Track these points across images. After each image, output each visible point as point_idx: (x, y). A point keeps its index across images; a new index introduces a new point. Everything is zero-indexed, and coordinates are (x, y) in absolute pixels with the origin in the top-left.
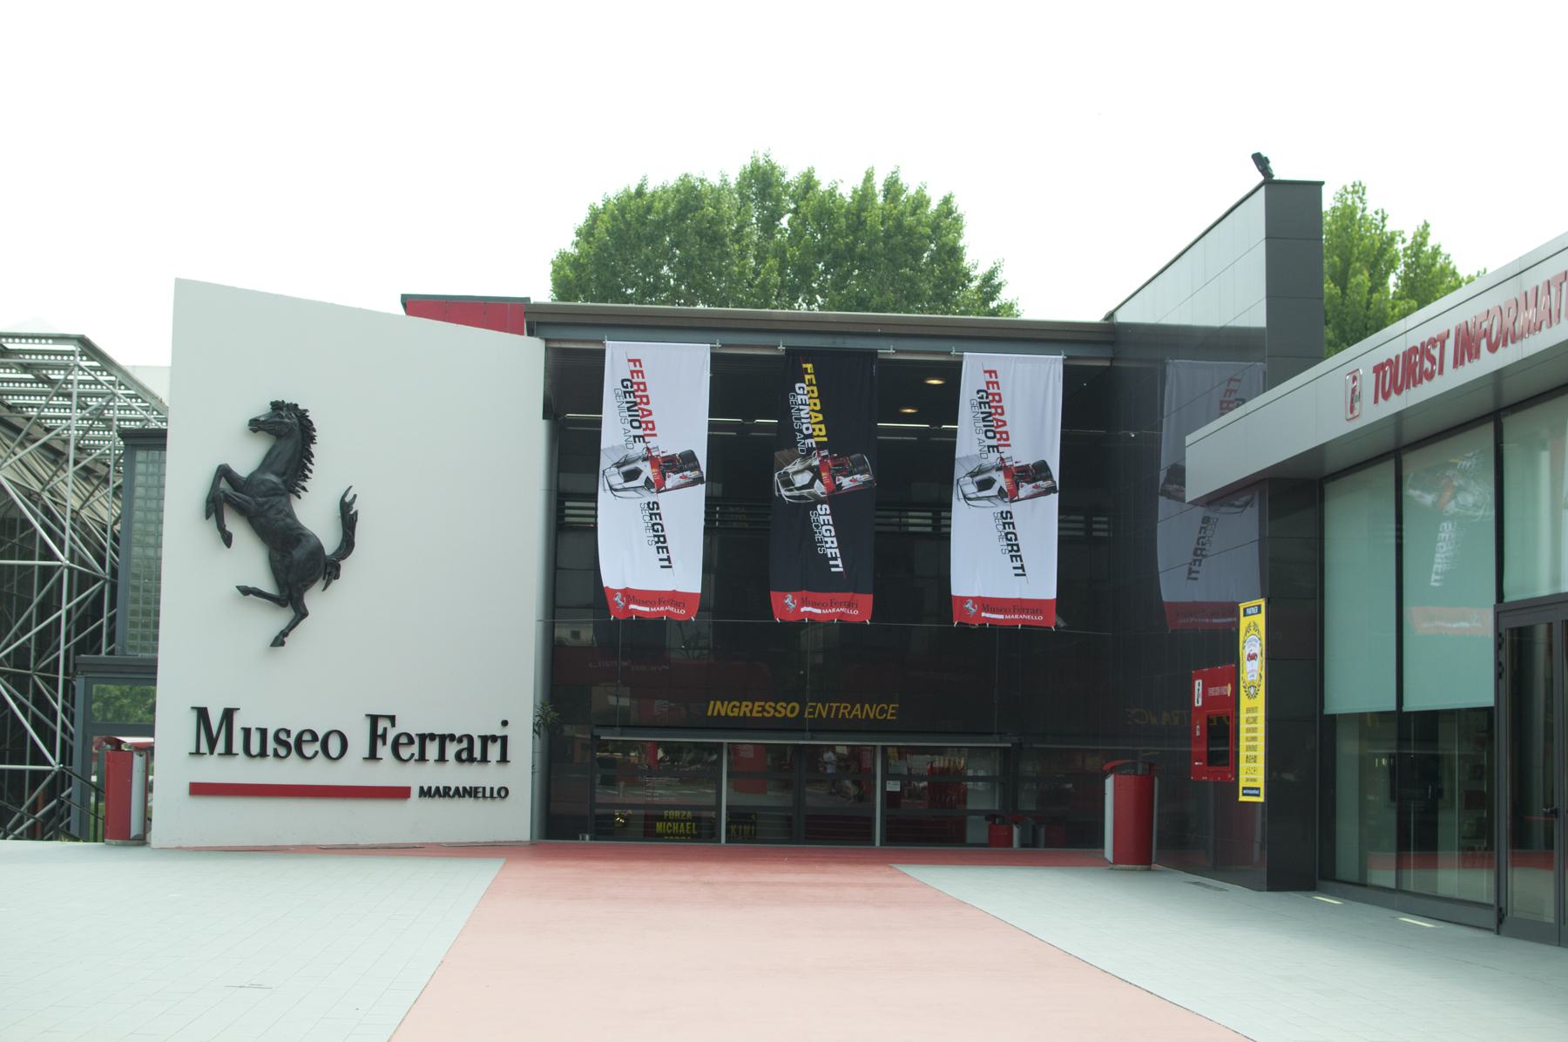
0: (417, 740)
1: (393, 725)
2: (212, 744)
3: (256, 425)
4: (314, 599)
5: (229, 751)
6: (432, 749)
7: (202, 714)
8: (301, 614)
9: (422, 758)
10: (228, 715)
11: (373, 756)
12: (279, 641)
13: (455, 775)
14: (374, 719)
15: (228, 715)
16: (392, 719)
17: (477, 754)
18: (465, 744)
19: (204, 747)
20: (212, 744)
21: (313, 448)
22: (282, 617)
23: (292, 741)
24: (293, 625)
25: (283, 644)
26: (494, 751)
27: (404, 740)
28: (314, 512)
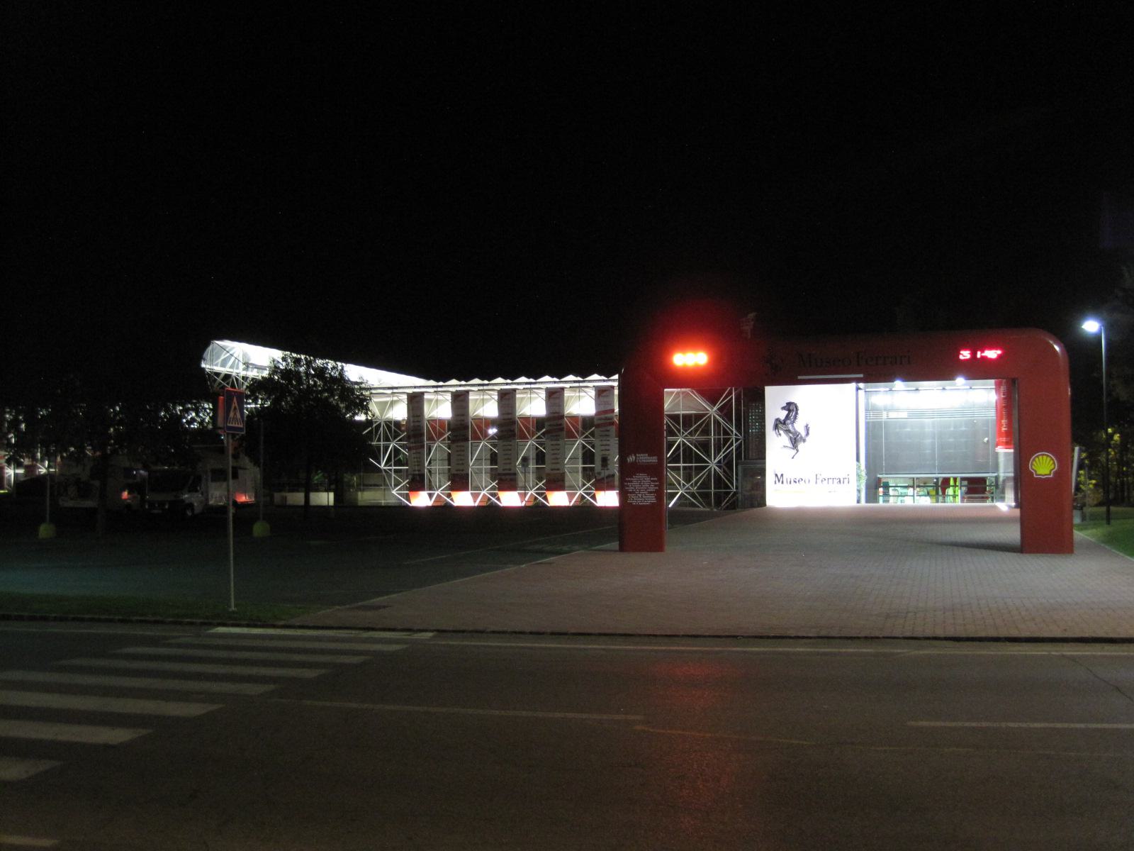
2: (779, 481)
3: (783, 408)
4: (801, 446)
7: (776, 475)
8: (798, 451)
10: (782, 475)
15: (782, 475)
17: (842, 482)
19: (777, 482)
20: (779, 481)
28: (799, 426)
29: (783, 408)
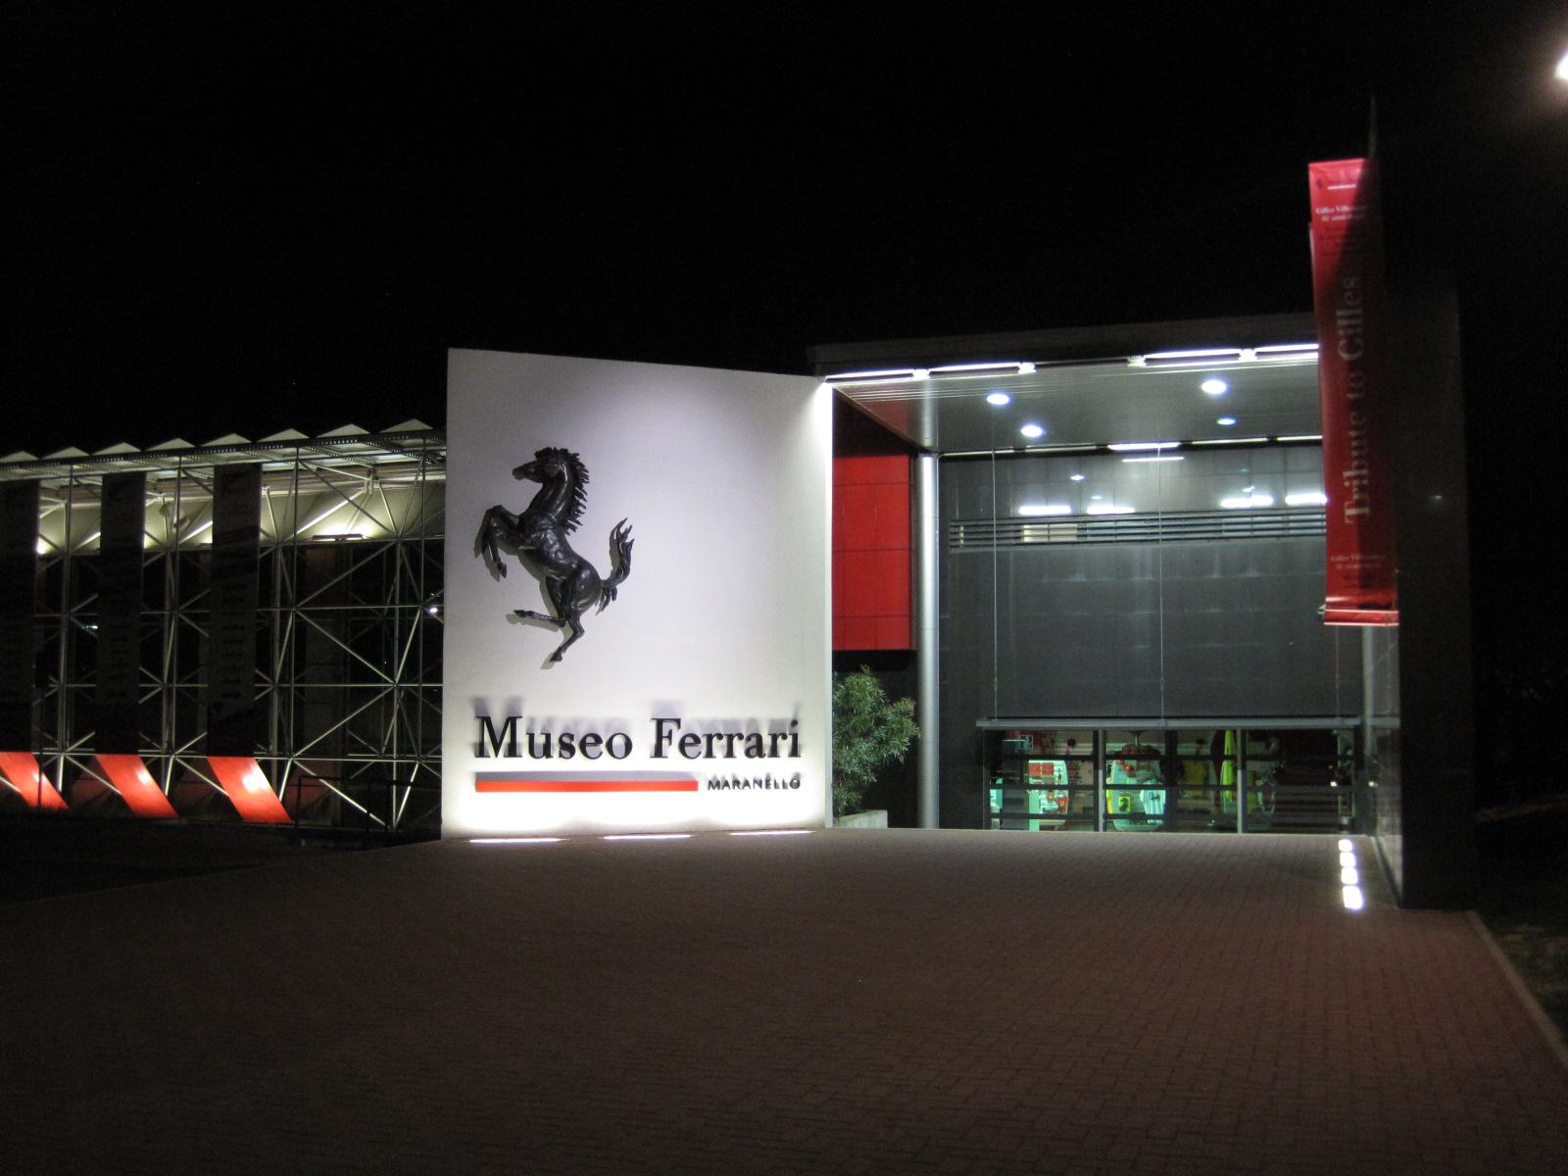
0: (704, 741)
1: (679, 727)
4: (589, 618)
5: (512, 751)
6: (719, 746)
7: (486, 721)
8: (577, 632)
9: (709, 754)
10: (511, 721)
11: (658, 752)
12: (556, 657)
13: (743, 766)
14: (660, 723)
16: (678, 722)
18: (754, 740)
21: (586, 487)
22: (558, 637)
23: (576, 744)
25: (560, 659)
26: (785, 746)
27: (689, 740)
28: (589, 542)
29: (522, 472)
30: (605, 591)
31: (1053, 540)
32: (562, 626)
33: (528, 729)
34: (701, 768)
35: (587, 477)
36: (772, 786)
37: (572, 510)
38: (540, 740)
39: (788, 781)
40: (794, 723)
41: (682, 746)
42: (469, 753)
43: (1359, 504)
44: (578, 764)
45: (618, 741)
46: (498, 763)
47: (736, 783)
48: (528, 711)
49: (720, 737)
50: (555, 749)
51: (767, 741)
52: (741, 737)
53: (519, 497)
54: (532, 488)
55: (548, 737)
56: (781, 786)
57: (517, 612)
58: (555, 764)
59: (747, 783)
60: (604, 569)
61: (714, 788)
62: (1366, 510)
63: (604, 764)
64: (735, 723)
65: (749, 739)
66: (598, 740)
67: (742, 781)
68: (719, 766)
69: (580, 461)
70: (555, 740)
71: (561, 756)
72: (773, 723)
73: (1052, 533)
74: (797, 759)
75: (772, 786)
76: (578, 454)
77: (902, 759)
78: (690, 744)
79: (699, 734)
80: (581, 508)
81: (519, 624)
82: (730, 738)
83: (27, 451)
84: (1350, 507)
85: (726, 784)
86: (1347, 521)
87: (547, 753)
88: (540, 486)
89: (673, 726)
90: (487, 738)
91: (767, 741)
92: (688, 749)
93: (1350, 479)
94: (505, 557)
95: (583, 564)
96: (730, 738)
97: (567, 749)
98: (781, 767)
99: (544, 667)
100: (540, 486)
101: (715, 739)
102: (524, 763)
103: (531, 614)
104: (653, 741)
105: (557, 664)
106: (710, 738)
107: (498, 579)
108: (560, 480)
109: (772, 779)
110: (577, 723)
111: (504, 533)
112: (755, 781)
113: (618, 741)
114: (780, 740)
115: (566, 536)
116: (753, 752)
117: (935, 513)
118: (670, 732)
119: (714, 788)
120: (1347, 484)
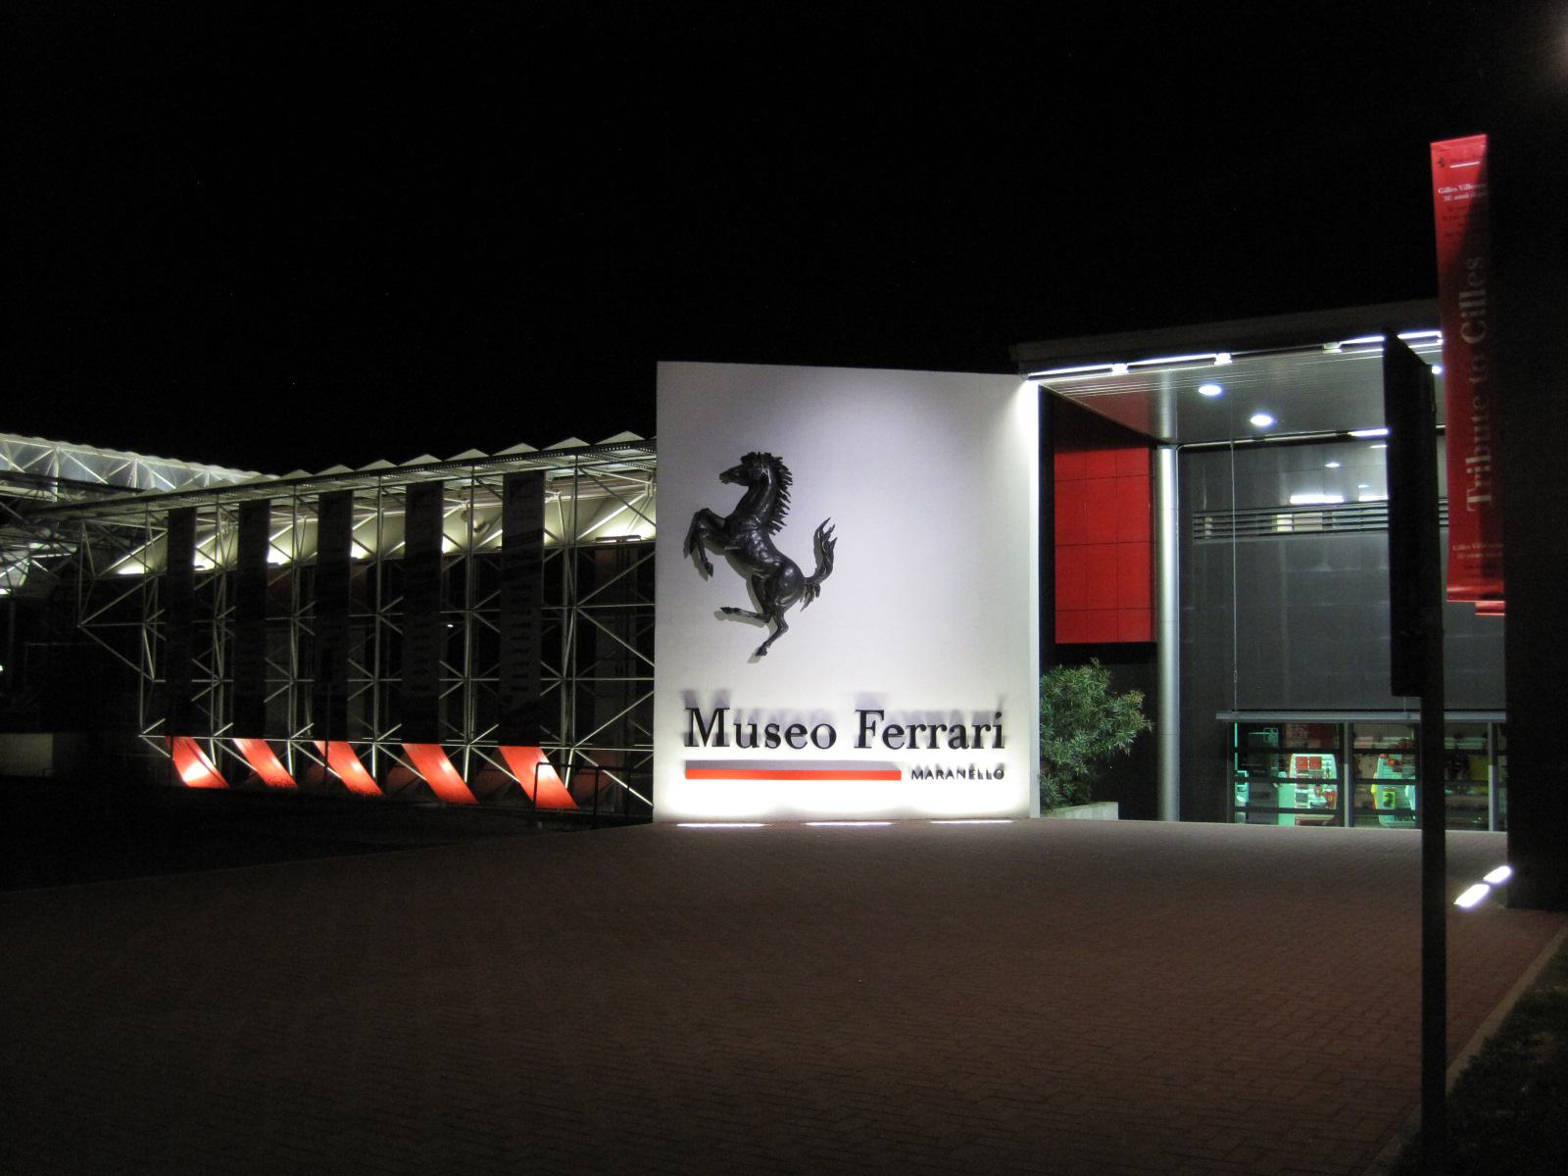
0: (907, 732)
4: (794, 614)
6: (922, 737)
7: (695, 712)
8: (781, 628)
9: (913, 745)
10: (720, 712)
11: (862, 743)
12: (761, 651)
13: (947, 756)
14: (863, 714)
16: (881, 713)
18: (957, 732)
21: (789, 489)
23: (781, 734)
24: (773, 637)
25: (765, 653)
26: (989, 737)
28: (794, 542)
29: (728, 476)
30: (809, 588)
31: (1297, 529)
32: (767, 621)
33: (736, 720)
34: (904, 758)
35: (790, 480)
36: (976, 776)
37: (774, 517)
38: (747, 730)
39: (992, 772)
40: (998, 715)
41: (886, 737)
42: (680, 742)
43: (1481, 491)
44: (783, 753)
45: (823, 732)
46: (706, 752)
47: (940, 773)
48: (734, 703)
49: (923, 728)
50: (762, 739)
51: (970, 732)
52: (944, 728)
53: (726, 499)
54: (739, 491)
55: (754, 727)
56: (985, 776)
57: (724, 609)
58: (761, 753)
59: (950, 774)
60: (808, 567)
61: (917, 778)
62: (1487, 498)
63: (809, 753)
64: (938, 714)
65: (952, 730)
66: (803, 731)
67: (945, 771)
68: (924, 756)
69: (784, 464)
70: (761, 731)
71: (767, 745)
72: (977, 715)
73: (1297, 522)
74: (935, 750)
75: (976, 776)
76: (781, 458)
77: (1128, 751)
78: (894, 735)
79: (903, 727)
80: (785, 509)
81: (726, 620)
82: (934, 729)
83: (255, 470)
84: (1472, 494)
85: (930, 774)
86: (1469, 509)
87: (754, 742)
88: (745, 489)
89: (877, 717)
90: (696, 728)
91: (970, 732)
92: (890, 740)
93: (1472, 466)
94: (710, 555)
95: (786, 563)
96: (934, 729)
97: (773, 739)
98: (985, 757)
99: (750, 662)
100: (745, 489)
101: (918, 731)
102: (732, 752)
103: (737, 610)
104: (857, 731)
105: (763, 658)
106: (913, 729)
107: (706, 579)
108: (764, 483)
109: (976, 769)
110: (783, 713)
111: (710, 534)
112: (958, 772)
113: (823, 732)
114: (983, 731)
115: (770, 535)
116: (957, 743)
117: (1175, 505)
118: (874, 723)
119: (917, 778)
120: (1469, 471)
